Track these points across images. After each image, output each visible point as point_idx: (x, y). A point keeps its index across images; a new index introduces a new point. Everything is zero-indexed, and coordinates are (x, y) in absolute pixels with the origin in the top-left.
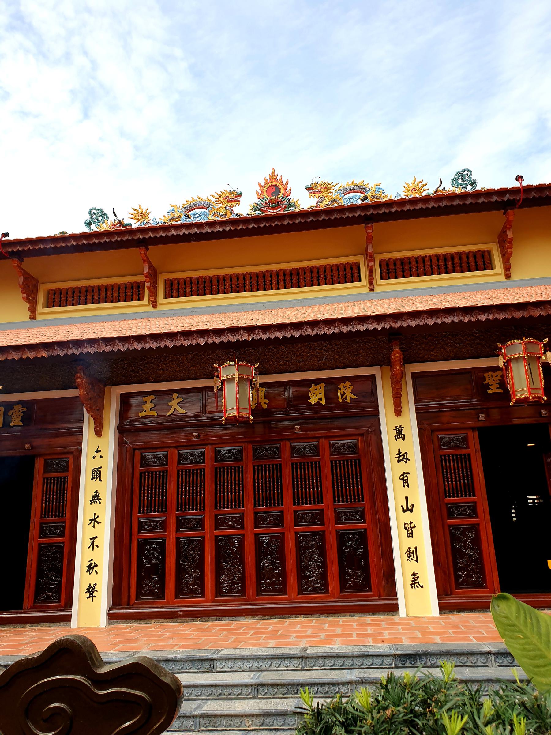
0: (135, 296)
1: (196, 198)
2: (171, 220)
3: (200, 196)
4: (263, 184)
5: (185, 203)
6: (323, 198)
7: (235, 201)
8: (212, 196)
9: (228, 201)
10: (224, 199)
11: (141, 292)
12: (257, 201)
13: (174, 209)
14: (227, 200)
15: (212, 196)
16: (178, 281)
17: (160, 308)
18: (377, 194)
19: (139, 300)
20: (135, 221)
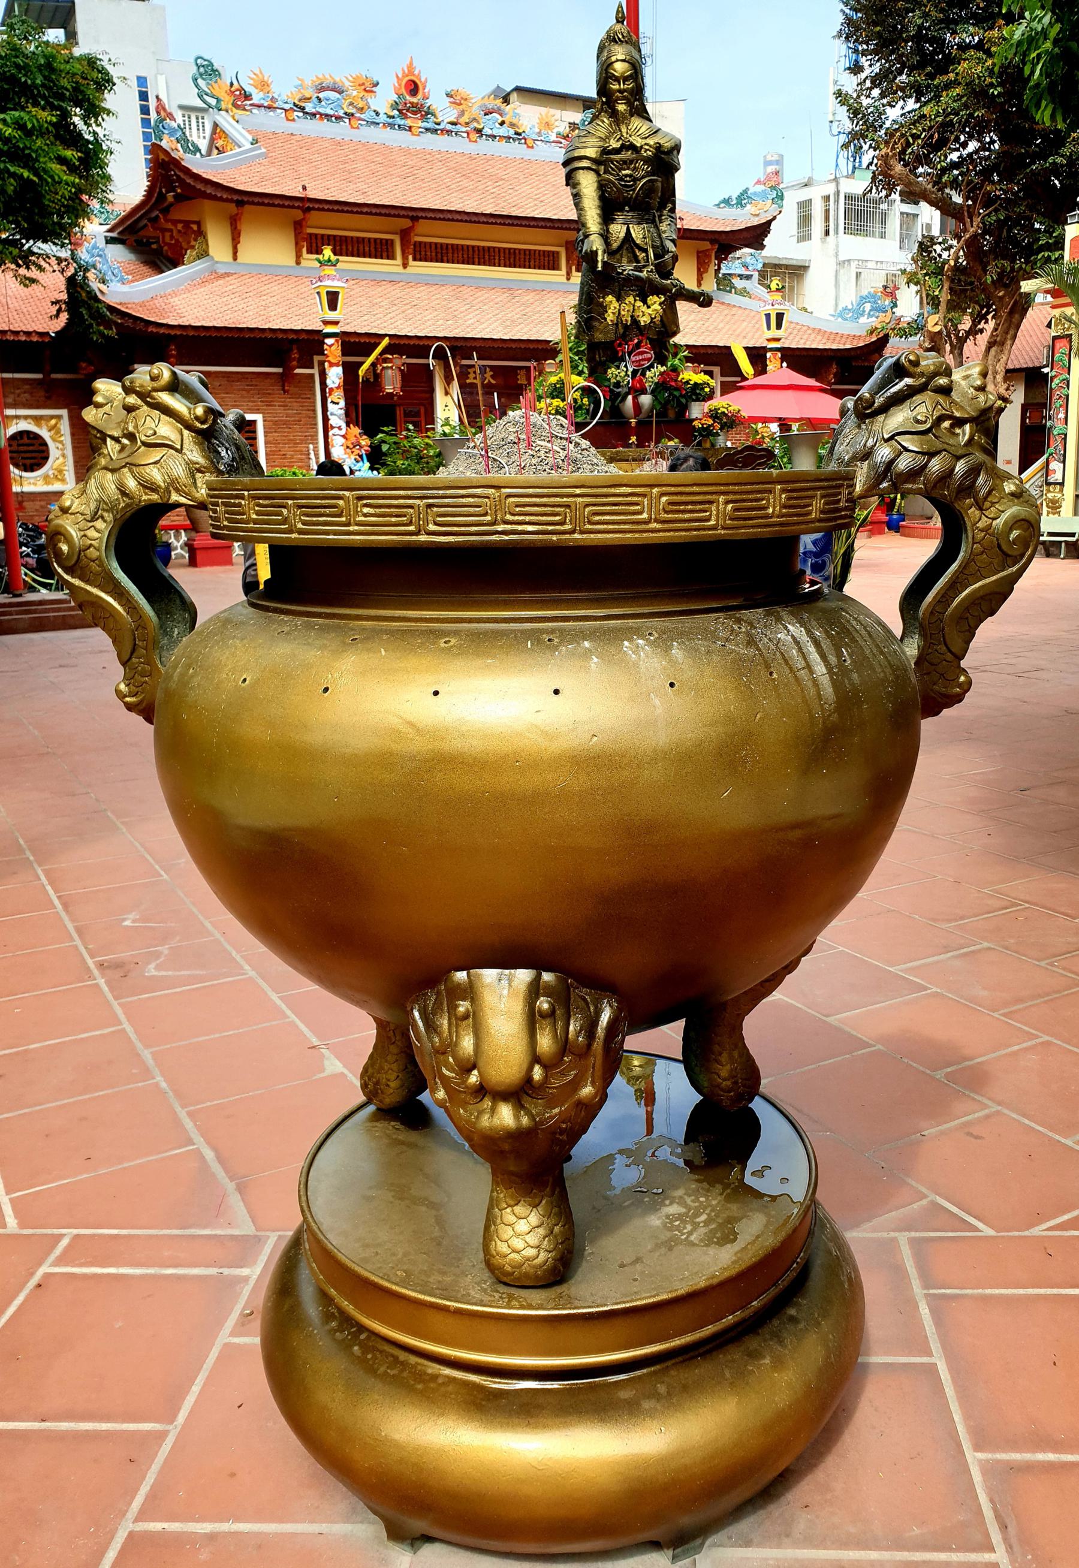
0: (385, 254)
1: (328, 76)
2: (300, 100)
3: (333, 76)
4: (400, 76)
5: (315, 79)
6: (462, 114)
7: (372, 92)
8: (347, 78)
9: (365, 90)
10: (359, 85)
11: (390, 250)
12: (395, 97)
13: (301, 85)
14: (363, 87)
15: (347, 78)
16: (420, 243)
17: (409, 270)
18: (515, 121)
19: (388, 258)
20: (256, 91)
